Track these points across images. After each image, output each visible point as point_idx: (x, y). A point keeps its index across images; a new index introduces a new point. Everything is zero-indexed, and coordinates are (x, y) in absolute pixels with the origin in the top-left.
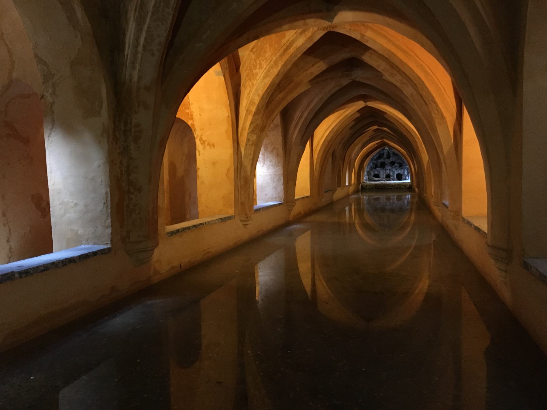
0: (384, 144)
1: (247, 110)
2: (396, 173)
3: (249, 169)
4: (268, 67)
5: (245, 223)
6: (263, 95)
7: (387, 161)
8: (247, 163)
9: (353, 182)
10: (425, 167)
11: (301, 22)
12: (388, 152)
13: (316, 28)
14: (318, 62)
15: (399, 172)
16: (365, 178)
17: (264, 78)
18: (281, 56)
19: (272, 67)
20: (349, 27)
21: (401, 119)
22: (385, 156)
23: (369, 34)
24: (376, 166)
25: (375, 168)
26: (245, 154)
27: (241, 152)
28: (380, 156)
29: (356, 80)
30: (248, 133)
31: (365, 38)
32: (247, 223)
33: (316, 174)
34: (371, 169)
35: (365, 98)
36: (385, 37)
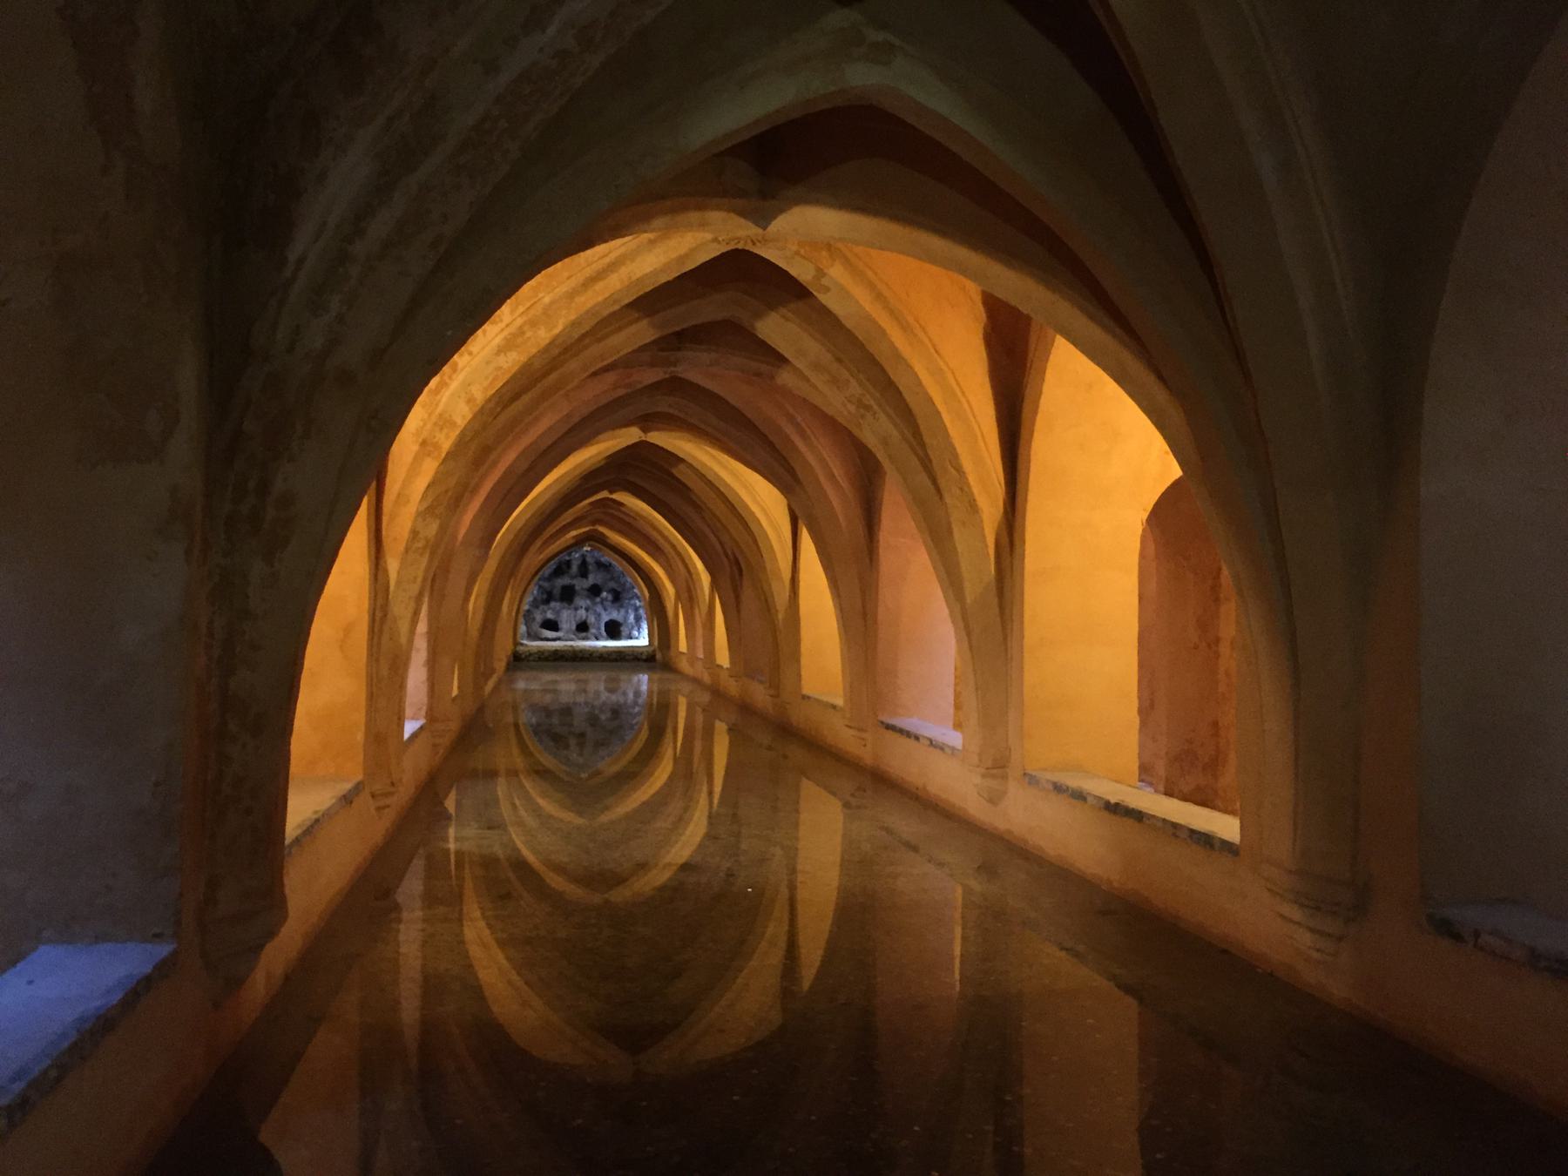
1: (424, 443)
2: (605, 618)
3: (404, 627)
4: (519, 321)
5: (381, 803)
6: (489, 400)
7: (581, 584)
10: (780, 616)
11: (694, 216)
12: (583, 557)
13: (709, 236)
14: (637, 320)
15: (615, 615)
16: (523, 629)
17: (501, 350)
18: (571, 295)
19: (533, 324)
20: (795, 248)
21: (727, 485)
22: (574, 568)
23: (837, 272)
24: (548, 598)
25: (547, 601)
26: (398, 583)
27: (386, 571)
28: (561, 570)
30: (419, 514)
31: (824, 281)
32: (387, 801)
34: (535, 604)
35: (647, 421)
36: (871, 286)
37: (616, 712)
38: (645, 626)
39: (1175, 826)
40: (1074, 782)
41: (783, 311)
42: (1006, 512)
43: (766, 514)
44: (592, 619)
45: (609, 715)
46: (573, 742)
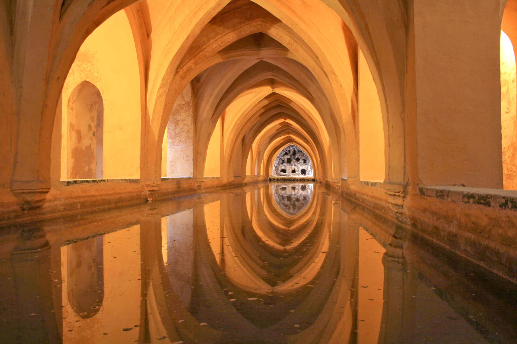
0: (291, 140)
2: (301, 168)
8: (155, 128)
9: (262, 174)
22: (291, 153)
24: (283, 162)
25: (283, 163)
29: (265, 60)
33: (227, 156)
34: (279, 164)
35: (272, 83)
37: (305, 198)
41: (275, 26)
42: (354, 90)
44: (296, 169)
45: (302, 198)
46: (291, 207)
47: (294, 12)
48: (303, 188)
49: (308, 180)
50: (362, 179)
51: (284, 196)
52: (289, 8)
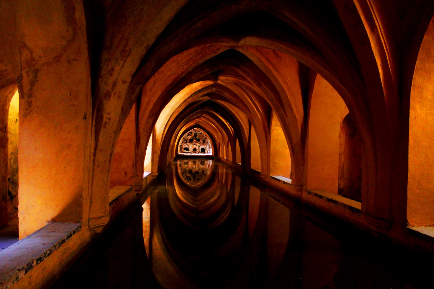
2: (201, 147)
5: (137, 193)
38: (211, 150)
39: (345, 205)
40: (321, 194)
43: (242, 119)
44: (197, 148)
47: (270, 63)
48: (203, 163)
49: (208, 158)
50: (309, 188)
51: (187, 169)
52: (267, 59)
